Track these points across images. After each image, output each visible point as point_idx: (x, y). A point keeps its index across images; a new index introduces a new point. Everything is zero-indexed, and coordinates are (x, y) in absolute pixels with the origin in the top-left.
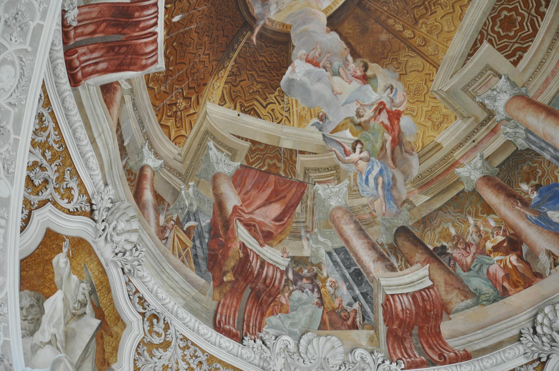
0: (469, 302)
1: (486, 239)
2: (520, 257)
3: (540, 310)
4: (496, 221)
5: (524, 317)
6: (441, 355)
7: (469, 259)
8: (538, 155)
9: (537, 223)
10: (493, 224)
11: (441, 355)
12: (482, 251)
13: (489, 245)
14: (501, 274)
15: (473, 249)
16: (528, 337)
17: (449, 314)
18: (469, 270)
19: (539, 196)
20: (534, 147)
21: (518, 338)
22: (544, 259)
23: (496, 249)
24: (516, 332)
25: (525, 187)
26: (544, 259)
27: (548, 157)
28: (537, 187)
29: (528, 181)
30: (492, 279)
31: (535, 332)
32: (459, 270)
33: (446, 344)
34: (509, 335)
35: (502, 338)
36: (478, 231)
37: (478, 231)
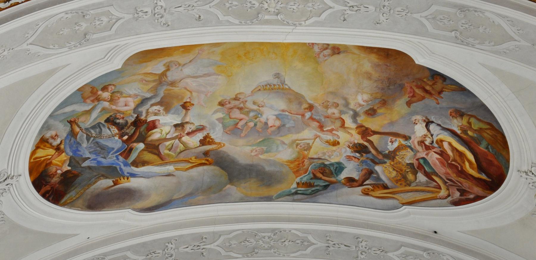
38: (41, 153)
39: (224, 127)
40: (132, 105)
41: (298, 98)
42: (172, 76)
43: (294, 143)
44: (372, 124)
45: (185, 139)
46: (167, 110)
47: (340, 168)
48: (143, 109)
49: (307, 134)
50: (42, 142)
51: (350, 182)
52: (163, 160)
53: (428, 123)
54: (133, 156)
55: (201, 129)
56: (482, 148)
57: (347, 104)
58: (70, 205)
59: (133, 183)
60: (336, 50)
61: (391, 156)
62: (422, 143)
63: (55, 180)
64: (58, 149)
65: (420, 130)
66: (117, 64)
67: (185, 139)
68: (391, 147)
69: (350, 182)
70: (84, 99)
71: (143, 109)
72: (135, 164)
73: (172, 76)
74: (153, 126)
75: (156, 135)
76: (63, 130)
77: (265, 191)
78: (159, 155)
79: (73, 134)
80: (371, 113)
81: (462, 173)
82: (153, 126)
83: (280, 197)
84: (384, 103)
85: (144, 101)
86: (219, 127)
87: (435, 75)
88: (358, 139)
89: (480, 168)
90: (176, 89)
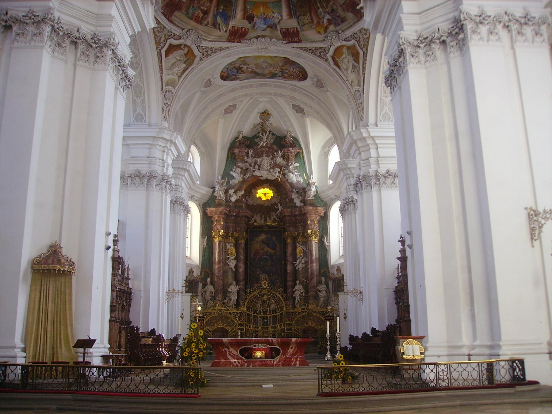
0: (185, 13)
1: (203, 6)
2: (203, 17)
3: (192, 30)
4: (209, 5)
5: (189, 27)
6: (169, 17)
7: (196, 6)
8: (232, 6)
9: (214, 15)
10: (208, 5)
11: (169, 17)
12: (199, 7)
13: (202, 8)
14: (196, 15)
15: (199, 5)
16: (185, 31)
17: (180, 11)
18: (193, 7)
19: (222, 12)
20: (234, 3)
21: (183, 29)
22: (206, 22)
23: (202, 10)
24: (184, 28)
25: (222, 7)
26: (206, 22)
27: (233, 8)
28: (223, 10)
29: (224, 7)
30: (194, 14)
31: (187, 32)
32: (192, 6)
33: (172, 16)
34: (182, 27)
35: (180, 26)
36: (204, 3)
37: (204, 3)
38: (222, 74)
39: (256, 68)
40: (238, 65)
41: (270, 64)
42: (245, 60)
43: (268, 70)
44: (283, 68)
45: (249, 70)
46: (245, 66)
47: (277, 74)
48: (240, 66)
49: (271, 69)
50: (222, 72)
51: (279, 76)
52: (244, 73)
53: (293, 69)
54: (239, 73)
55: (251, 68)
56: (303, 73)
57: (278, 65)
58: (227, 81)
59: (239, 76)
60: (276, 57)
61: (287, 73)
62: (292, 71)
63: (224, 77)
64: (225, 73)
65: (292, 70)
66: (235, 59)
67: (249, 70)
68: (287, 71)
69: (279, 76)
70: (230, 65)
71: (240, 66)
72: (239, 74)
73: (245, 60)
74: (242, 68)
75: (243, 69)
76: (226, 70)
77: (264, 77)
78: (244, 72)
79: (227, 70)
80: (283, 66)
81: (300, 77)
82: (242, 68)
83: (267, 78)
84: (285, 65)
85: (241, 64)
86: (255, 68)
87: (294, 62)
88: (281, 70)
89: (303, 76)
90: (247, 62)
